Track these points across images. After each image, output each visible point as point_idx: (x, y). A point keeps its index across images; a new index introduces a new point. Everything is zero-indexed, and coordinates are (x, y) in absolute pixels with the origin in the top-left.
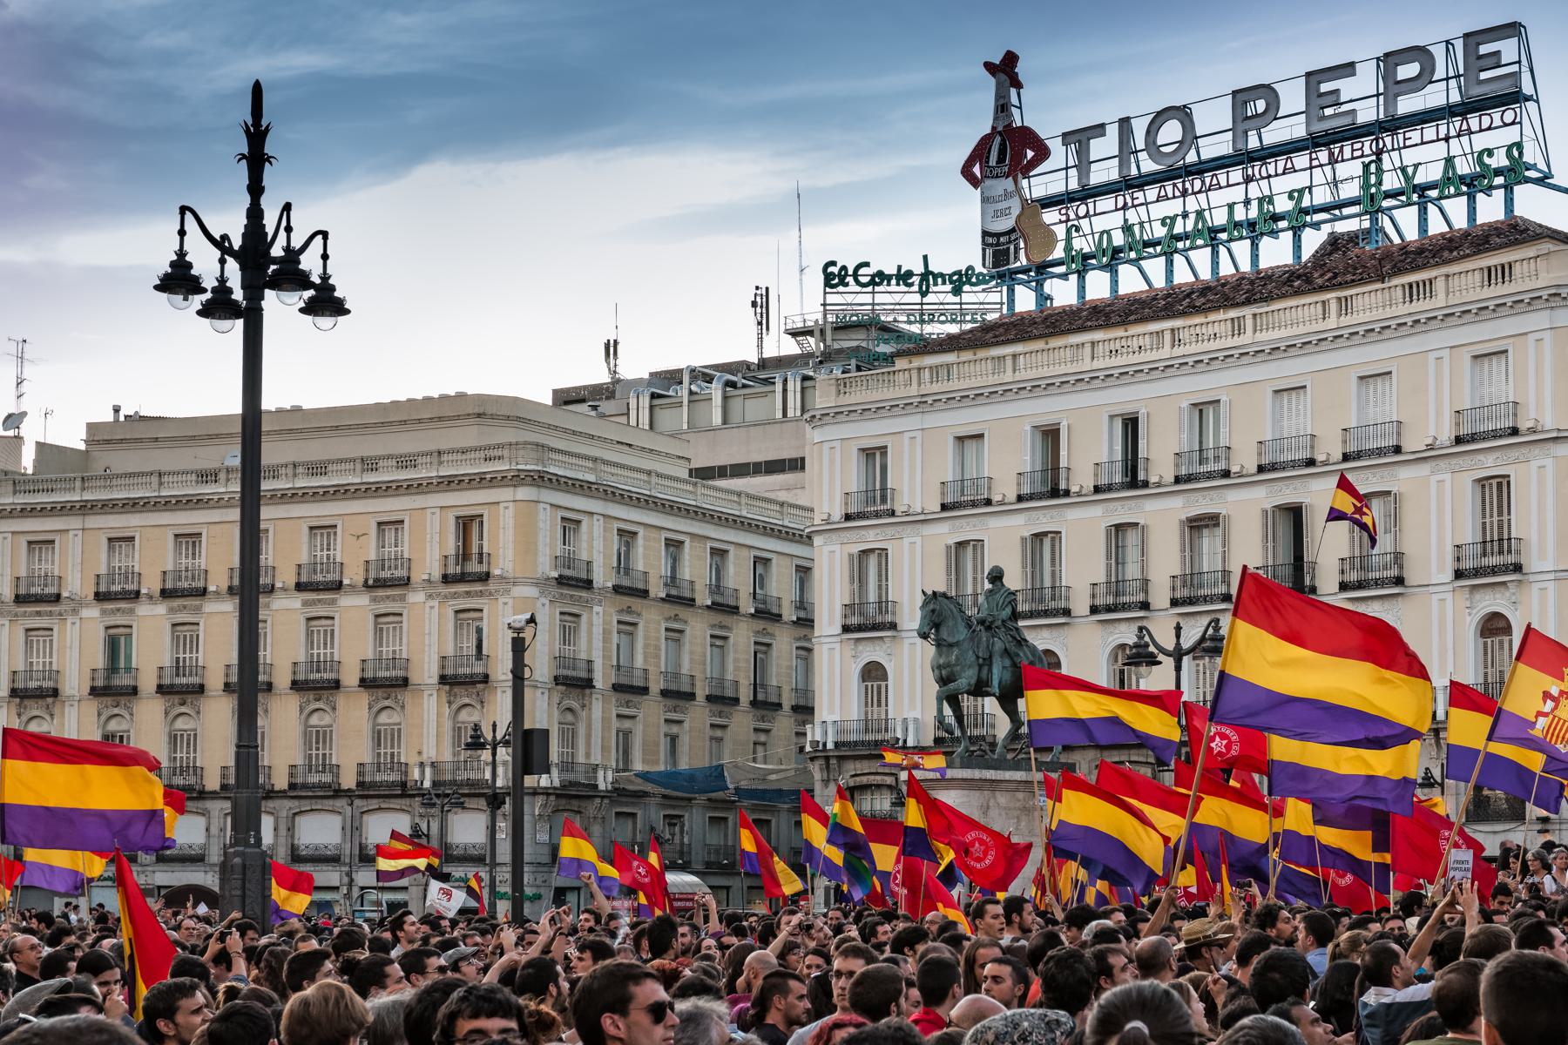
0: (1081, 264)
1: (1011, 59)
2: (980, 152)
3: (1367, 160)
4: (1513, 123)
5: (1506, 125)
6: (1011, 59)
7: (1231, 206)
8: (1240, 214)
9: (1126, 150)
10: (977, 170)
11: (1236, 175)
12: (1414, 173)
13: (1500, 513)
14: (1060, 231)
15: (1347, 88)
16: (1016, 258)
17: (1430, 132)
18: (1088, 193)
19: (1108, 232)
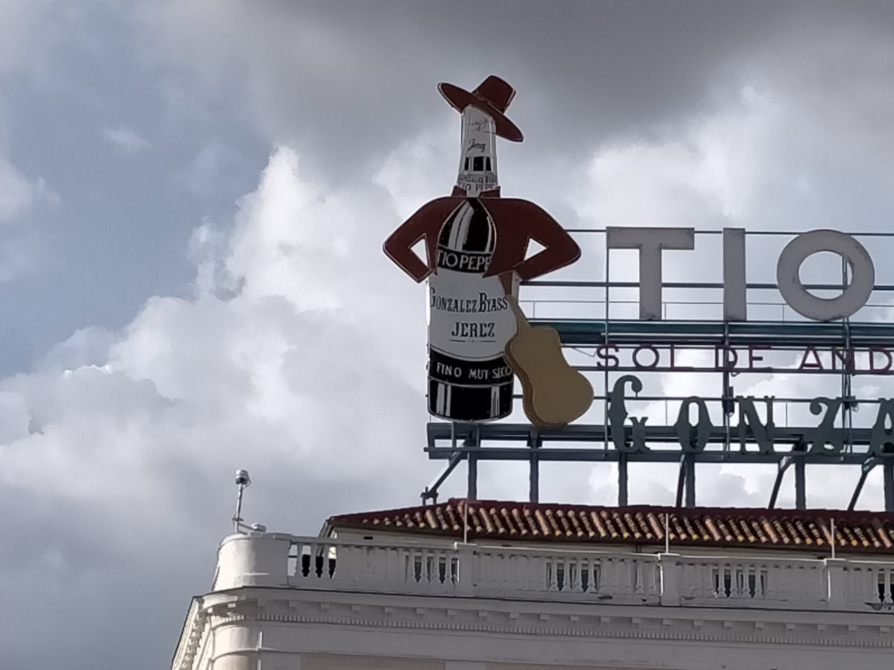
0: (629, 444)
1: (494, 96)
2: (430, 221)
6: (494, 96)
9: (735, 282)
10: (420, 249)
14: (598, 382)
16: (506, 409)
18: (655, 332)
19: (701, 402)
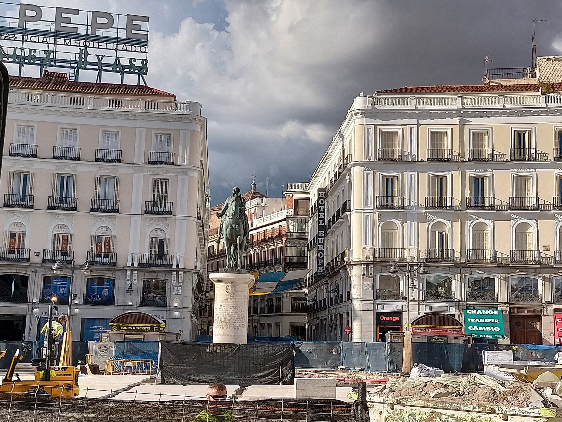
3: (82, 48)
4: (144, 52)
5: (141, 52)
7: (15, 49)
8: (19, 53)
11: (19, 37)
12: (102, 58)
13: (166, 193)
15: (74, 18)
17: (110, 46)
